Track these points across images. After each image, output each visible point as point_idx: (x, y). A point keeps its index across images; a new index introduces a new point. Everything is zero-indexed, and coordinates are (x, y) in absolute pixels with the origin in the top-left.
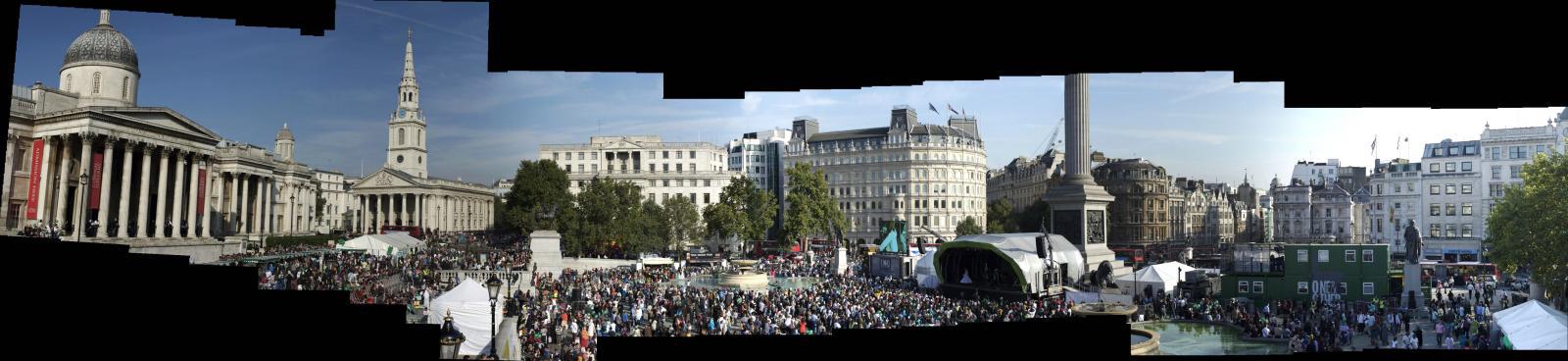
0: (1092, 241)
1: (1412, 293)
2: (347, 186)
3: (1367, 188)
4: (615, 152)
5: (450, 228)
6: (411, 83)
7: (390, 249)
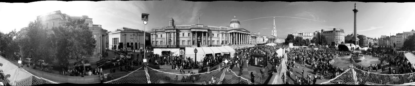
1: (394, 51)
2: (267, 38)
3: (389, 39)
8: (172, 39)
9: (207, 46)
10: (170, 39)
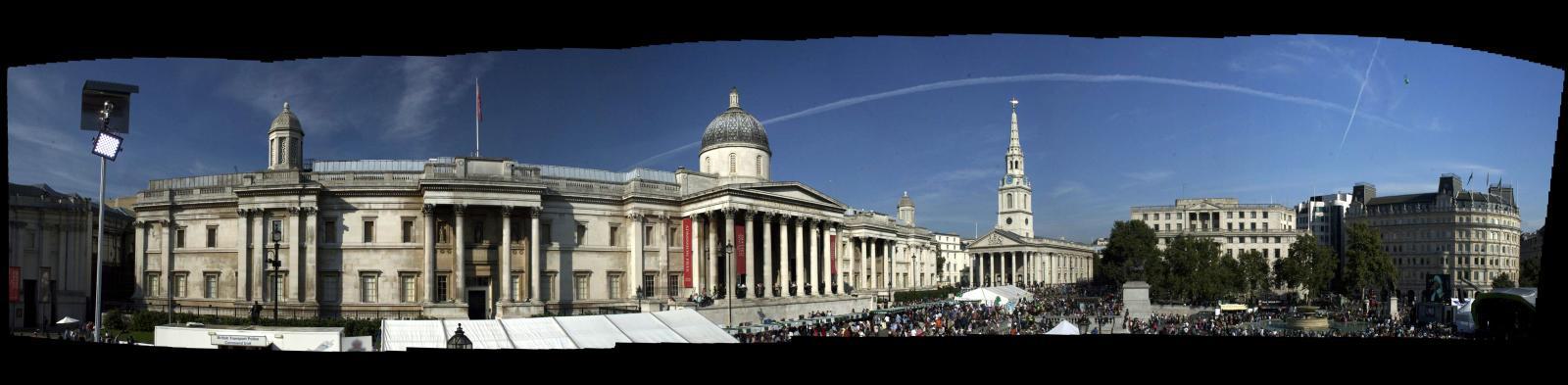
2: (963, 246)
4: (1198, 213)
5: (1054, 281)
6: (1016, 152)
8: (290, 260)
9: (533, 310)
10: (271, 256)
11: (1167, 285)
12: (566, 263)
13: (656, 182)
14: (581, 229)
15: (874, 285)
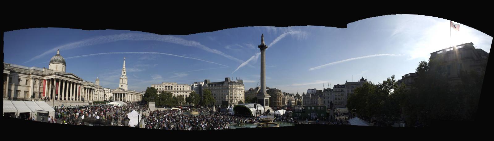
0: (266, 105)
1: (331, 116)
2: (110, 91)
5: (132, 101)
6: (124, 70)
7: (118, 104)
11: (159, 103)
12: (16, 88)
13: (38, 70)
14: (19, 80)
15: (88, 99)
